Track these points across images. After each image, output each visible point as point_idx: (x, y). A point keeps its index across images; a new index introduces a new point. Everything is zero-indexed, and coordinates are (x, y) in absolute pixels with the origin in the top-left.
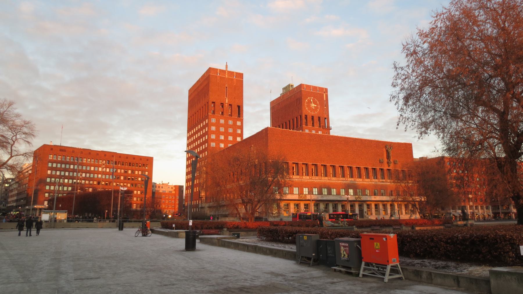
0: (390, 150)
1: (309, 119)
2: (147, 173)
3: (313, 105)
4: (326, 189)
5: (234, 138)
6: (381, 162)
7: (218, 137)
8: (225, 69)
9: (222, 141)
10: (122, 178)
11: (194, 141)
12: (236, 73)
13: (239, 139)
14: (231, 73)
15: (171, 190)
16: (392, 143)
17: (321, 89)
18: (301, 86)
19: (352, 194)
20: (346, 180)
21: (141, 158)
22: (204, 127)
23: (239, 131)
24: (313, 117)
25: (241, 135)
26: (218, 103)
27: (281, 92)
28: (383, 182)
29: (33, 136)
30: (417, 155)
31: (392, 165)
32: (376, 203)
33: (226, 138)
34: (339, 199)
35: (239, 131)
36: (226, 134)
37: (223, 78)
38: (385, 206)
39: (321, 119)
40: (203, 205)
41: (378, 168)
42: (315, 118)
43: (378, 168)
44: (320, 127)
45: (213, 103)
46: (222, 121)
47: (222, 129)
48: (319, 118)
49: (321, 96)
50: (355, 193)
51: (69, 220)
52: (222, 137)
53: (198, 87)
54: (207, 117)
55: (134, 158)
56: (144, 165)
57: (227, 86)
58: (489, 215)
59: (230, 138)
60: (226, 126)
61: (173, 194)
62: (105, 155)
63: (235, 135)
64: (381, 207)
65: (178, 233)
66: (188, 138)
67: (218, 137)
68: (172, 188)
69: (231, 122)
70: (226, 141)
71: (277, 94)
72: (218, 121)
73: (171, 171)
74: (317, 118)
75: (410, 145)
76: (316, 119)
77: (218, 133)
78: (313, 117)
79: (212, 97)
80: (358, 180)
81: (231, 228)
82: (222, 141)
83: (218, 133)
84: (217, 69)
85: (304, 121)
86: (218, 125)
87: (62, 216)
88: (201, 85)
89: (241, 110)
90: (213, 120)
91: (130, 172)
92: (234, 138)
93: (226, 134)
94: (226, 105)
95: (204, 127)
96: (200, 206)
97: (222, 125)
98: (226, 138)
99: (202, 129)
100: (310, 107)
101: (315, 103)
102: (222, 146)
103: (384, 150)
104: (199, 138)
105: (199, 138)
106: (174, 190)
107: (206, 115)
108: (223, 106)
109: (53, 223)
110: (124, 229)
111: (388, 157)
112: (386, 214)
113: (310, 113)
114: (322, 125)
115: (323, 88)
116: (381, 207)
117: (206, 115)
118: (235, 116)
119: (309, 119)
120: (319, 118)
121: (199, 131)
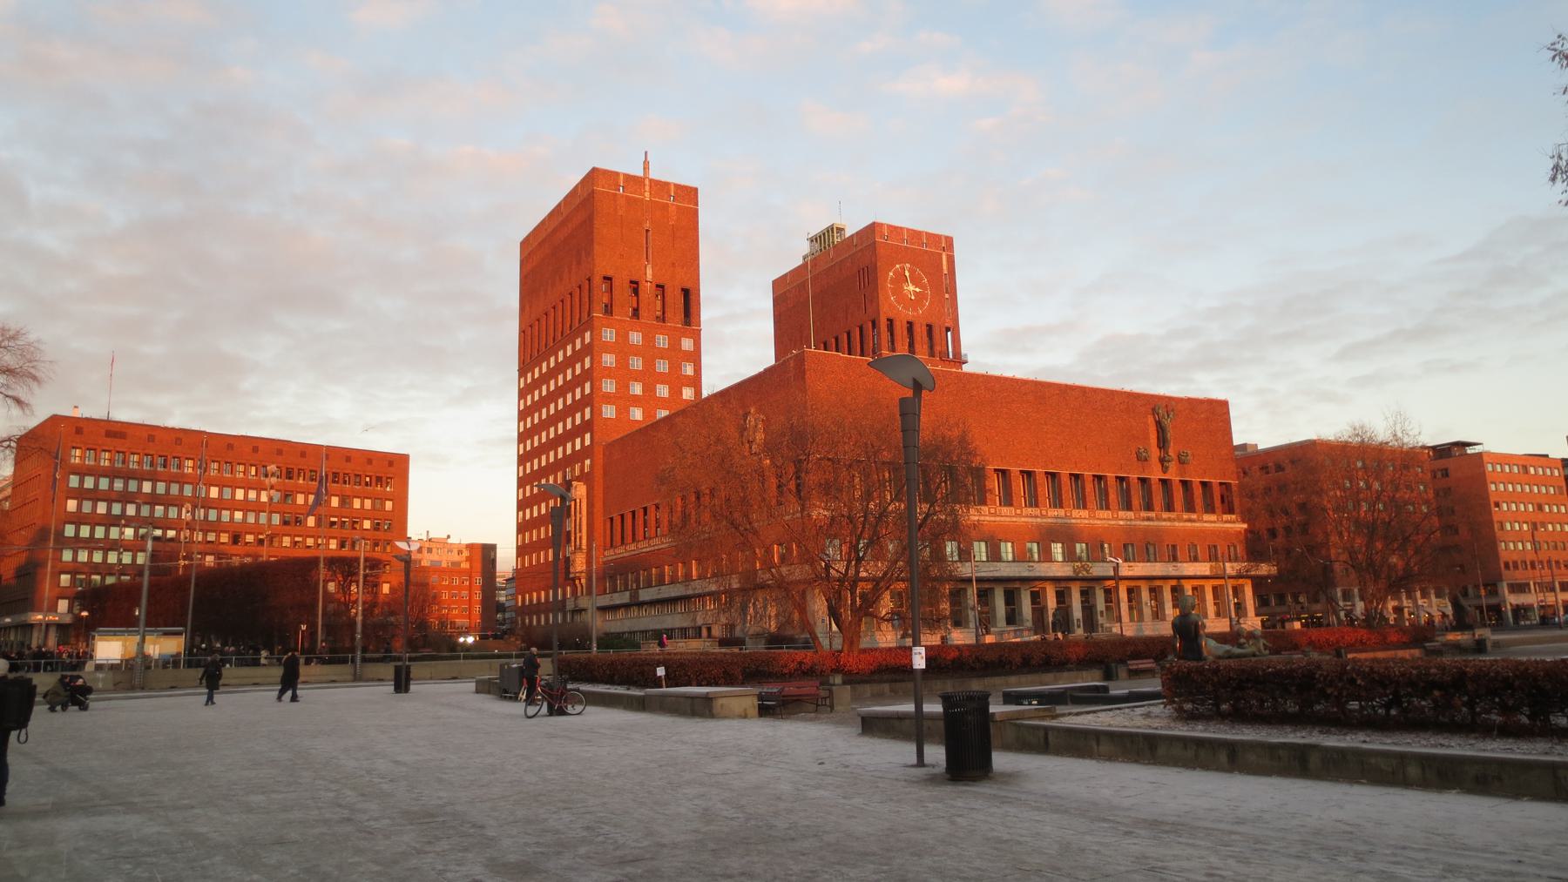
0: (1167, 422)
1: (901, 330)
2: (389, 505)
3: (911, 288)
4: (983, 545)
6: (1142, 459)
7: (623, 386)
8: (639, 173)
9: (636, 401)
10: (311, 521)
11: (544, 402)
12: (677, 186)
13: (688, 393)
14: (661, 187)
15: (456, 558)
16: (1171, 399)
17: (934, 239)
18: (873, 228)
19: (1060, 558)
20: (1042, 516)
21: (370, 457)
22: (578, 357)
23: (689, 370)
24: (910, 324)
25: (696, 382)
26: (621, 283)
27: (805, 248)
28: (1148, 519)
29: (35, 378)
30: (1242, 434)
31: (1173, 465)
32: (1133, 584)
33: (649, 389)
34: (1026, 574)
35: (689, 370)
36: (649, 377)
37: (636, 200)
38: (1155, 592)
39: (936, 331)
40: (584, 602)
41: (1134, 476)
43: (1134, 476)
44: (932, 354)
45: (608, 279)
46: (636, 338)
47: (636, 363)
48: (930, 327)
49: (933, 258)
50: (1070, 556)
51: (191, 658)
52: (637, 389)
53: (555, 231)
54: (588, 324)
55: (348, 459)
56: (379, 479)
57: (647, 225)
58: (1444, 615)
59: (663, 391)
60: (649, 352)
61: (461, 572)
62: (255, 449)
64: (1145, 595)
65: (708, 699)
66: (522, 394)
67: (623, 386)
68: (460, 552)
69: (662, 341)
71: (794, 254)
72: (623, 336)
73: (467, 499)
74: (925, 328)
75: (1224, 405)
76: (920, 333)
77: (624, 375)
78: (910, 324)
79: (604, 264)
80: (1075, 513)
81: (791, 675)
82: (636, 401)
83: (624, 375)
84: (617, 174)
85: (885, 335)
86: (623, 349)
87: (162, 646)
88: (563, 223)
89: (693, 304)
90: (609, 335)
91: (335, 502)
93: (649, 377)
94: (647, 289)
95: (578, 357)
96: (570, 605)
97: (636, 351)
98: (649, 389)
99: (570, 362)
100: (903, 294)
101: (916, 283)
102: (637, 414)
103: (1150, 420)
106: (469, 559)
107: (585, 317)
108: (636, 291)
109: (134, 676)
110: (413, 687)
111: (1162, 443)
112: (1158, 615)
113: (904, 314)
114: (937, 348)
115: (939, 237)
116: (1145, 595)
117: (585, 317)
118: (675, 319)
119: (901, 330)
120: (930, 327)
121: (560, 368)
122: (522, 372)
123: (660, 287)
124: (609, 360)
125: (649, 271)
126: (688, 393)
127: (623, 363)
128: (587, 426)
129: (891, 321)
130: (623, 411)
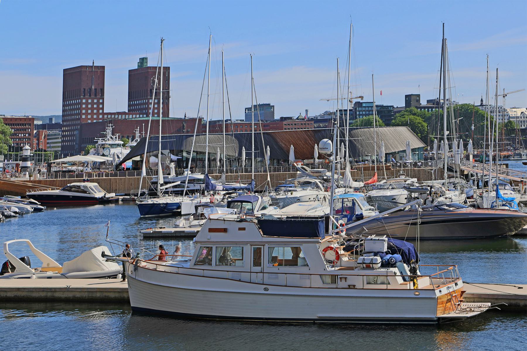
5: (98, 111)
25: (103, 109)
35: (101, 106)
36: (92, 109)
46: (90, 101)
60: (93, 104)
63: (98, 109)
70: (92, 114)
83: (87, 109)
93: (92, 109)
98: (92, 111)
123: (96, 89)
124: (84, 106)
126: (101, 111)
127: (87, 106)
128: (79, 119)
130: (86, 116)
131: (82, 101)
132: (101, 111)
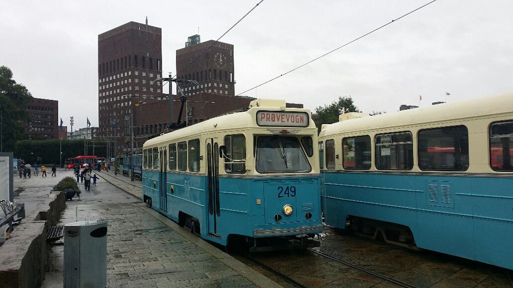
5: (155, 90)
36: (148, 86)
42: (222, 73)
44: (226, 80)
46: (144, 74)
48: (226, 72)
69: (151, 75)
70: (148, 92)
72: (140, 74)
92: (155, 90)
95: (127, 78)
104: (120, 87)
105: (120, 87)
120: (226, 72)
122: (100, 77)
123: (151, 59)
125: (148, 55)
126: (159, 91)
129: (215, 70)
131: (133, 73)
132: (159, 91)
